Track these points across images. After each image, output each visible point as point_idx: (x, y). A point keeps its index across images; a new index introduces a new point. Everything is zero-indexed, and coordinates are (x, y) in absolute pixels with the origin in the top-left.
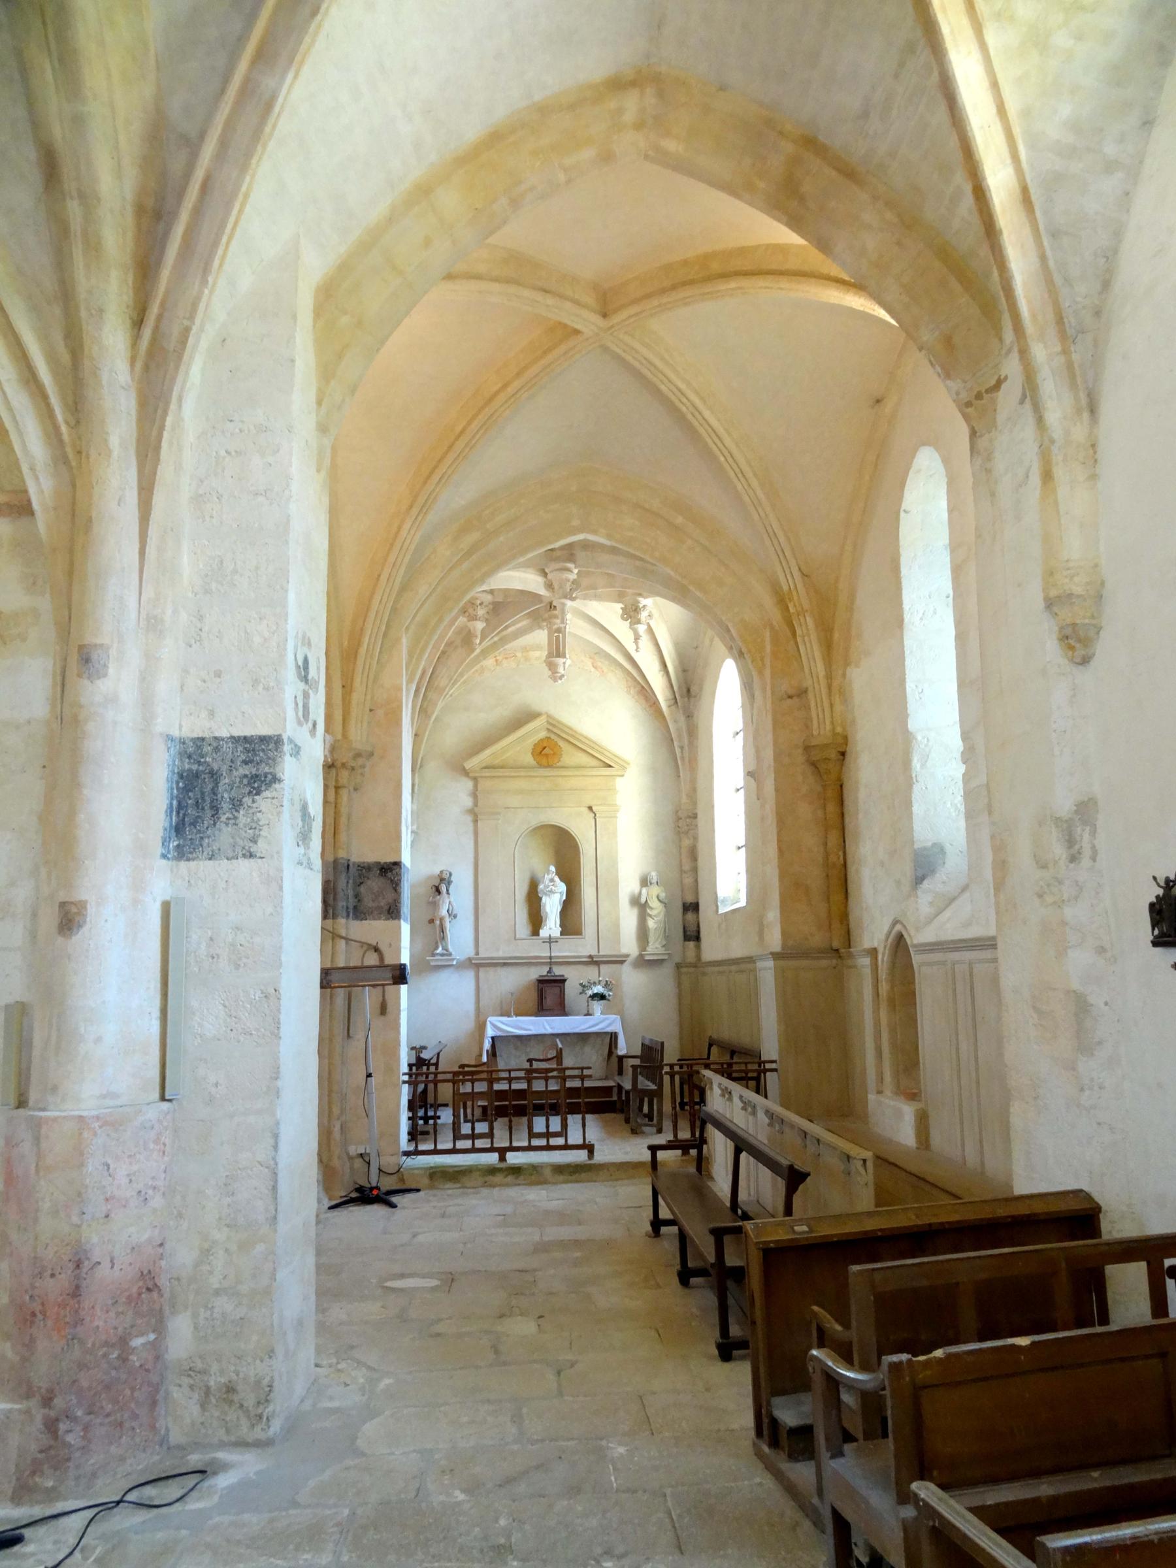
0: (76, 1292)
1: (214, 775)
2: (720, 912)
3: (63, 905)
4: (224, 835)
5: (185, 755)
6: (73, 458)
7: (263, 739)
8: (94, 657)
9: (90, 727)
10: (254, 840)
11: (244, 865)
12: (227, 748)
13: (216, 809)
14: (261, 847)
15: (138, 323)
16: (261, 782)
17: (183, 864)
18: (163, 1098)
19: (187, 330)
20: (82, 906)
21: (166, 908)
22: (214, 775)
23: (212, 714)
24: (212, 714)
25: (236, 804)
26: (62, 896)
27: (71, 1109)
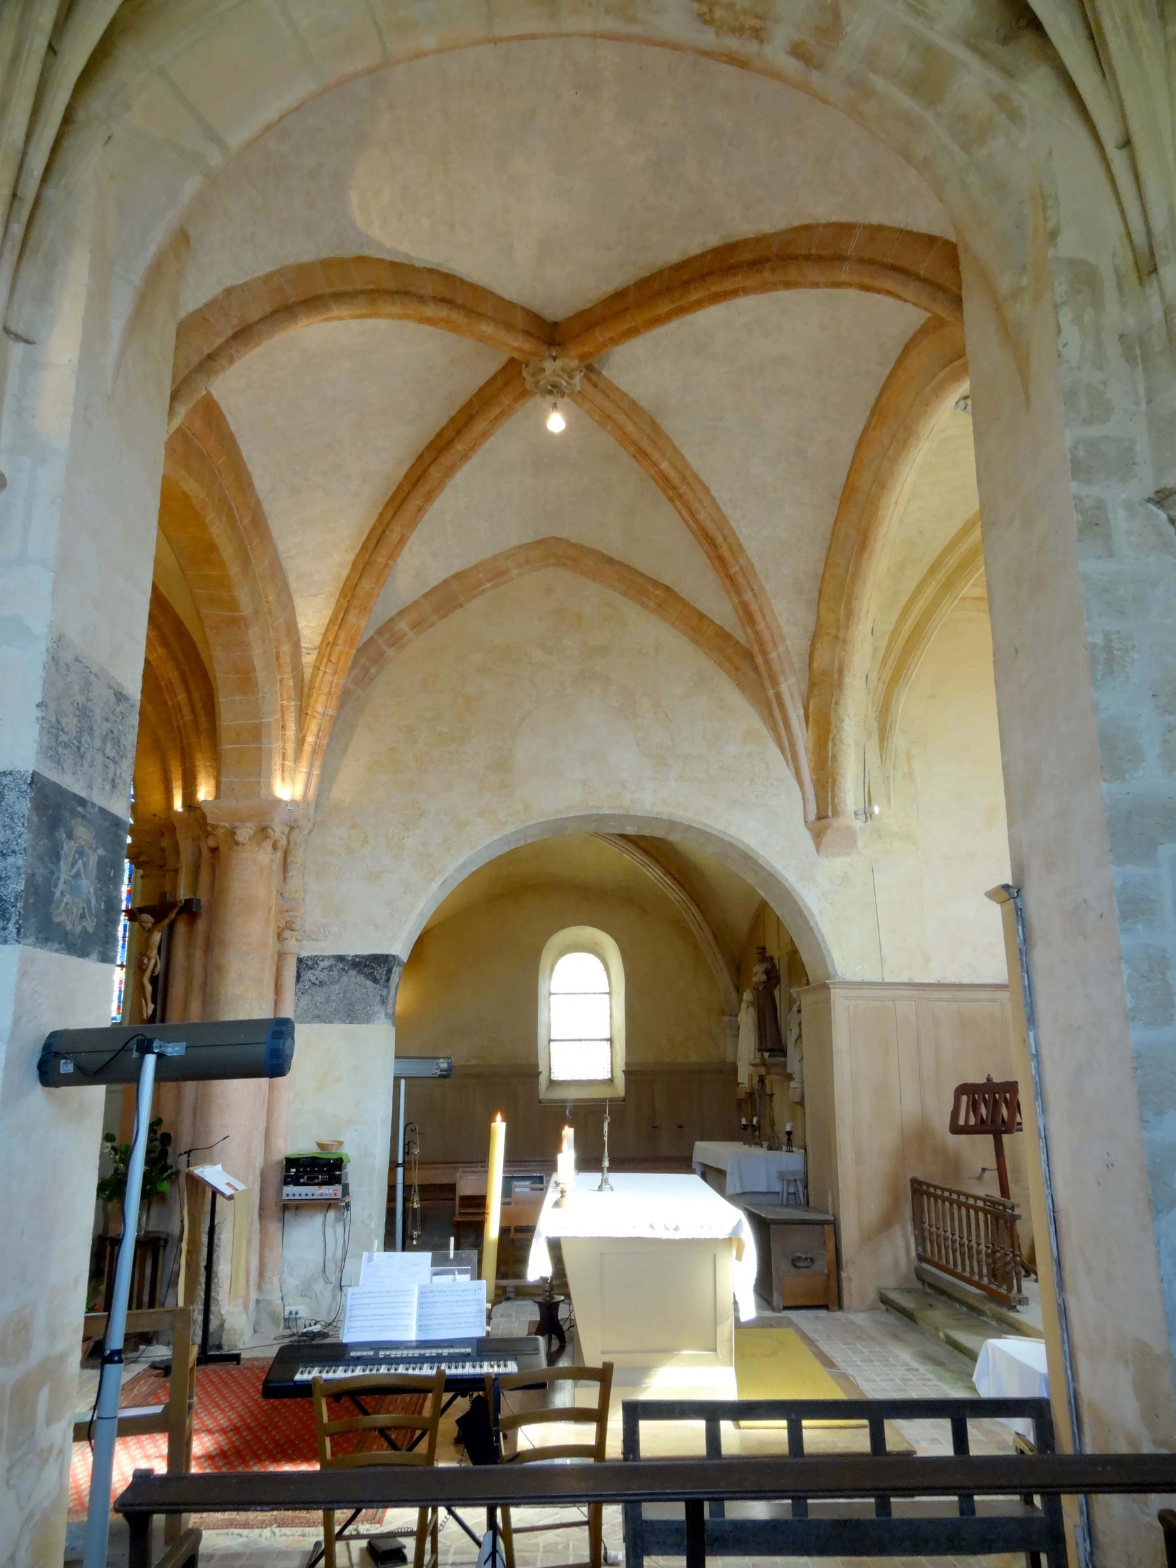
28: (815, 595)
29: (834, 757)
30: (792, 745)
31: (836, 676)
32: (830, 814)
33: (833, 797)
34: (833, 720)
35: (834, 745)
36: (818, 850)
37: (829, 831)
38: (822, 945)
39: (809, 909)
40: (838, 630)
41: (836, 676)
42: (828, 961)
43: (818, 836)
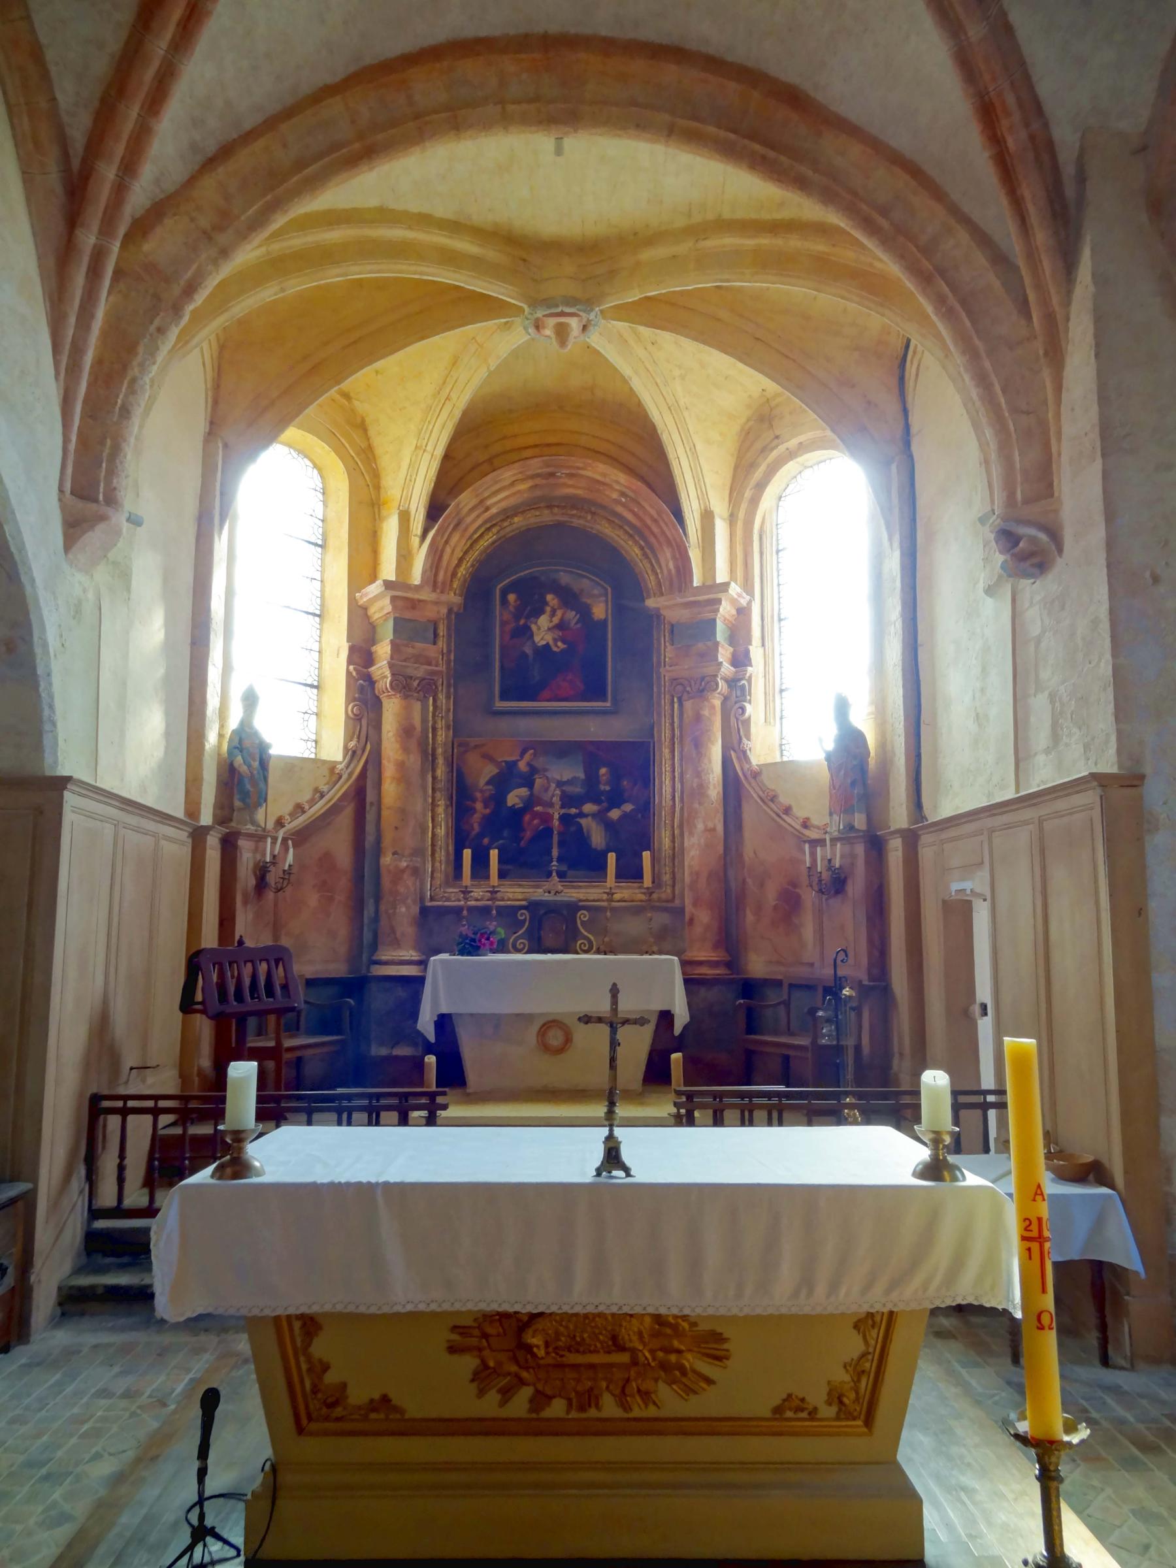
28: (211, 147)
29: (126, 412)
30: (77, 351)
31: (177, 290)
32: (101, 497)
33: (111, 472)
34: (141, 349)
35: (132, 391)
36: (67, 547)
37: (101, 527)
38: (46, 712)
39: (45, 645)
40: (219, 228)
41: (177, 290)
42: (47, 741)
43: (75, 527)
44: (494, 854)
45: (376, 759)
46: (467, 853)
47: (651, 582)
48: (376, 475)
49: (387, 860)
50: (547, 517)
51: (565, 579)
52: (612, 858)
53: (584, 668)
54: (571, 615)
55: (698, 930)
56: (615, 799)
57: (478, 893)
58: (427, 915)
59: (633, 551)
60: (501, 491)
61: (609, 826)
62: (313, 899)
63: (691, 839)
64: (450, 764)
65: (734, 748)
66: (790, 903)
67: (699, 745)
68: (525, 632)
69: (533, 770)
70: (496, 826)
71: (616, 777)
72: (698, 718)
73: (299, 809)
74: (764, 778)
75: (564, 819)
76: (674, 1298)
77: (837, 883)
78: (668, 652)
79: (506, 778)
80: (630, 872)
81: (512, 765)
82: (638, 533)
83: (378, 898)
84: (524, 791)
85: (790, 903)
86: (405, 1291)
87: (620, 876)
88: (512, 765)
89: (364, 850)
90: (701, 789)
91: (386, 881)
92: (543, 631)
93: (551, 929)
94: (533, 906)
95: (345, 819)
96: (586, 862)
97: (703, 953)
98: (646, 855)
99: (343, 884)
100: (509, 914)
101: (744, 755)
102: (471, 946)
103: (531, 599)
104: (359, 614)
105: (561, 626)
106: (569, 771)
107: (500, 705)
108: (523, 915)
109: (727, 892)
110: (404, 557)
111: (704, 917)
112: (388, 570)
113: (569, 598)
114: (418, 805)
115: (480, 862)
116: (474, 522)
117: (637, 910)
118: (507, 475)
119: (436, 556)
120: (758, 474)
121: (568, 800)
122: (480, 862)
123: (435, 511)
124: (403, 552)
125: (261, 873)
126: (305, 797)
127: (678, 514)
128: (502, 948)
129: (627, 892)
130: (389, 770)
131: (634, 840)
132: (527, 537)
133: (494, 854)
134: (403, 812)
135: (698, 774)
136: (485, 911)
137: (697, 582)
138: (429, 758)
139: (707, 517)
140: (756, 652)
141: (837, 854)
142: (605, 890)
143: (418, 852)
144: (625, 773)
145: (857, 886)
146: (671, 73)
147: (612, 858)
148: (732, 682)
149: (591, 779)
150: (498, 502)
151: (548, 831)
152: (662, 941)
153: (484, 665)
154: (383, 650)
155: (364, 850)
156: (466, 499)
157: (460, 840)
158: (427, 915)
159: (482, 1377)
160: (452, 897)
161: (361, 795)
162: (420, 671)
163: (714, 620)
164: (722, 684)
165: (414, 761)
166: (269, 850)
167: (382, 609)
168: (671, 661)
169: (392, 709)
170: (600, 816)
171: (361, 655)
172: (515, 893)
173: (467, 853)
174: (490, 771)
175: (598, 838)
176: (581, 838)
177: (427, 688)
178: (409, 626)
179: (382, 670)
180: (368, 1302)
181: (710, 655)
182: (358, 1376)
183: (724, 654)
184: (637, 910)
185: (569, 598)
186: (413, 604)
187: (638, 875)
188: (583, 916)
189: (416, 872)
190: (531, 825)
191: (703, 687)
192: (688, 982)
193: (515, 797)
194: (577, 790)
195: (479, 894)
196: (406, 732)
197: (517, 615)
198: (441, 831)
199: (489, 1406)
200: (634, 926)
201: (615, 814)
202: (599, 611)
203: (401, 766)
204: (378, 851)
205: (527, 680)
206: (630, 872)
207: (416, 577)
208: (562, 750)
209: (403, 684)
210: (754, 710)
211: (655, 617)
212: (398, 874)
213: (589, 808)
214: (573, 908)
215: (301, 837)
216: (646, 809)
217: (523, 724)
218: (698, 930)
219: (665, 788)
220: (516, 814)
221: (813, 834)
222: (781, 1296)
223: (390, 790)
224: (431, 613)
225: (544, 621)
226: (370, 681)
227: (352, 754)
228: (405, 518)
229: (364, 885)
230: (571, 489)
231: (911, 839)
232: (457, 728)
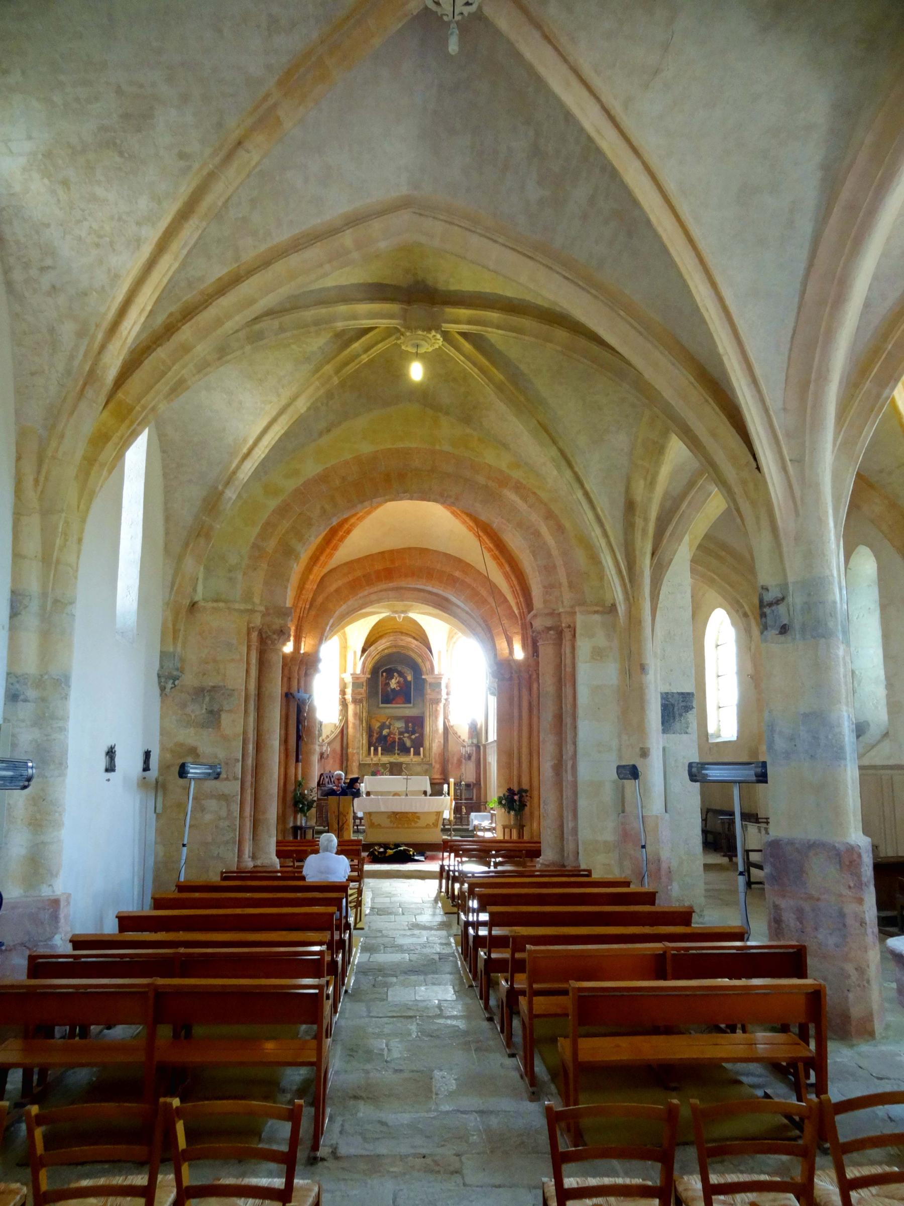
0: (659, 869)
1: (673, 705)
2: (711, 741)
3: (642, 749)
4: (677, 726)
5: (662, 698)
6: (632, 599)
7: (688, 694)
8: (646, 667)
9: (647, 691)
10: (687, 728)
11: (685, 736)
12: (676, 696)
13: (674, 718)
14: (689, 730)
15: (653, 554)
16: (688, 708)
17: (665, 735)
18: (666, 811)
19: (671, 560)
20: (649, 749)
21: (664, 749)
22: (673, 705)
23: (670, 684)
24: (670, 684)
25: (681, 715)
26: (641, 746)
27: (654, 813)
44: (380, 749)
45: (347, 721)
46: (372, 748)
47: (424, 669)
48: (346, 639)
49: (350, 750)
50: (394, 650)
51: (399, 668)
52: (412, 750)
53: (405, 694)
54: (401, 679)
55: (436, 770)
56: (413, 733)
57: (375, 759)
58: (361, 766)
59: (419, 661)
60: (382, 645)
61: (412, 741)
62: (331, 761)
63: (434, 743)
64: (367, 722)
65: (446, 718)
66: (460, 762)
67: (436, 718)
68: (388, 684)
69: (390, 724)
70: (380, 740)
71: (414, 725)
72: (436, 710)
73: (328, 737)
74: (455, 728)
75: (399, 739)
76: (414, 810)
77: (469, 757)
78: (428, 690)
79: (383, 727)
80: (417, 753)
81: (384, 723)
82: (419, 656)
83: (347, 760)
84: (387, 730)
85: (460, 762)
86: (383, 809)
87: (415, 754)
88: (384, 723)
89: (344, 748)
90: (437, 730)
91: (350, 756)
92: (393, 684)
93: (395, 769)
94: (391, 763)
95: (339, 738)
96: (405, 750)
97: (437, 776)
98: (422, 749)
99: (338, 757)
100: (384, 765)
101: (449, 721)
102: (374, 774)
103: (390, 673)
104: (342, 680)
105: (398, 682)
106: (400, 725)
107: (381, 705)
108: (388, 765)
109: (444, 759)
110: (355, 664)
111: (437, 766)
112: (350, 670)
113: (401, 674)
114: (358, 735)
115: (376, 750)
116: (374, 654)
117: (419, 764)
118: (383, 641)
119: (364, 664)
120: (454, 640)
121: (401, 733)
122: (376, 750)
123: (364, 651)
124: (356, 665)
125: (322, 755)
126: (329, 733)
127: (431, 652)
128: (382, 775)
129: (416, 759)
130: (350, 725)
131: (418, 744)
132: (390, 656)
133: (380, 749)
134: (354, 736)
135: (436, 726)
136: (377, 764)
137: (436, 672)
138: (361, 721)
139: (440, 652)
140: (452, 690)
141: (468, 749)
142: (411, 758)
143: (358, 748)
144: (416, 724)
145: (473, 758)
146: (422, 594)
147: (412, 750)
148: (446, 700)
149: (407, 726)
150: (380, 648)
151: (394, 742)
152: (426, 773)
153: (377, 693)
154: (349, 691)
155: (344, 748)
156: (372, 648)
157: (370, 744)
158: (361, 766)
159: (391, 822)
160: (368, 761)
161: (343, 733)
162: (359, 697)
163: (440, 684)
164: (443, 701)
165: (358, 722)
166: (324, 748)
167: (349, 679)
168: (429, 693)
169: (351, 708)
170: (409, 737)
171: (343, 693)
172: (386, 759)
173: (372, 748)
174: (378, 724)
175: (408, 744)
176: (404, 744)
177: (361, 701)
178: (356, 685)
179: (349, 697)
180: (379, 810)
181: (439, 693)
182: (376, 820)
183: (444, 691)
184: (419, 764)
185: (401, 674)
186: (358, 678)
187: (419, 754)
188: (404, 766)
189: (358, 754)
190: (390, 740)
191: (438, 701)
192: (431, 784)
193: (385, 732)
194: (403, 730)
195: (375, 760)
196: (355, 714)
197: (387, 678)
198: (364, 742)
199: (392, 825)
200: (419, 769)
201: (413, 737)
202: (409, 678)
203: (354, 724)
204: (347, 748)
205: (388, 698)
206: (417, 753)
207: (358, 671)
208: (398, 718)
209: (355, 701)
210: (451, 707)
211: (424, 680)
212: (353, 754)
213: (406, 735)
214: (401, 764)
215: (329, 744)
216: (422, 735)
217: (387, 711)
218: (436, 770)
219: (427, 729)
220: (386, 737)
221: (465, 744)
222: (426, 810)
223: (351, 730)
224: (362, 680)
225: (393, 681)
226: (344, 699)
227: (341, 721)
228: (355, 653)
229: (344, 759)
230: (401, 643)
231: (485, 746)
232: (369, 712)
